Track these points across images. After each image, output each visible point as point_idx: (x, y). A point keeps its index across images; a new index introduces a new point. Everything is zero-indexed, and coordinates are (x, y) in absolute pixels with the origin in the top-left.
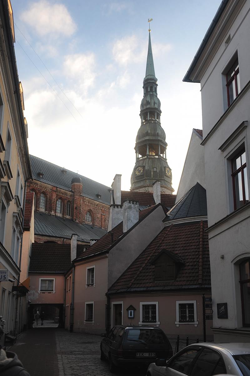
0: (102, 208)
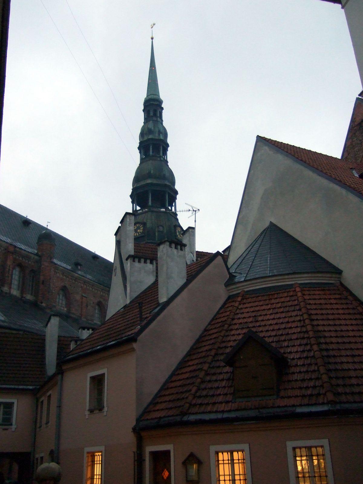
0: (82, 285)
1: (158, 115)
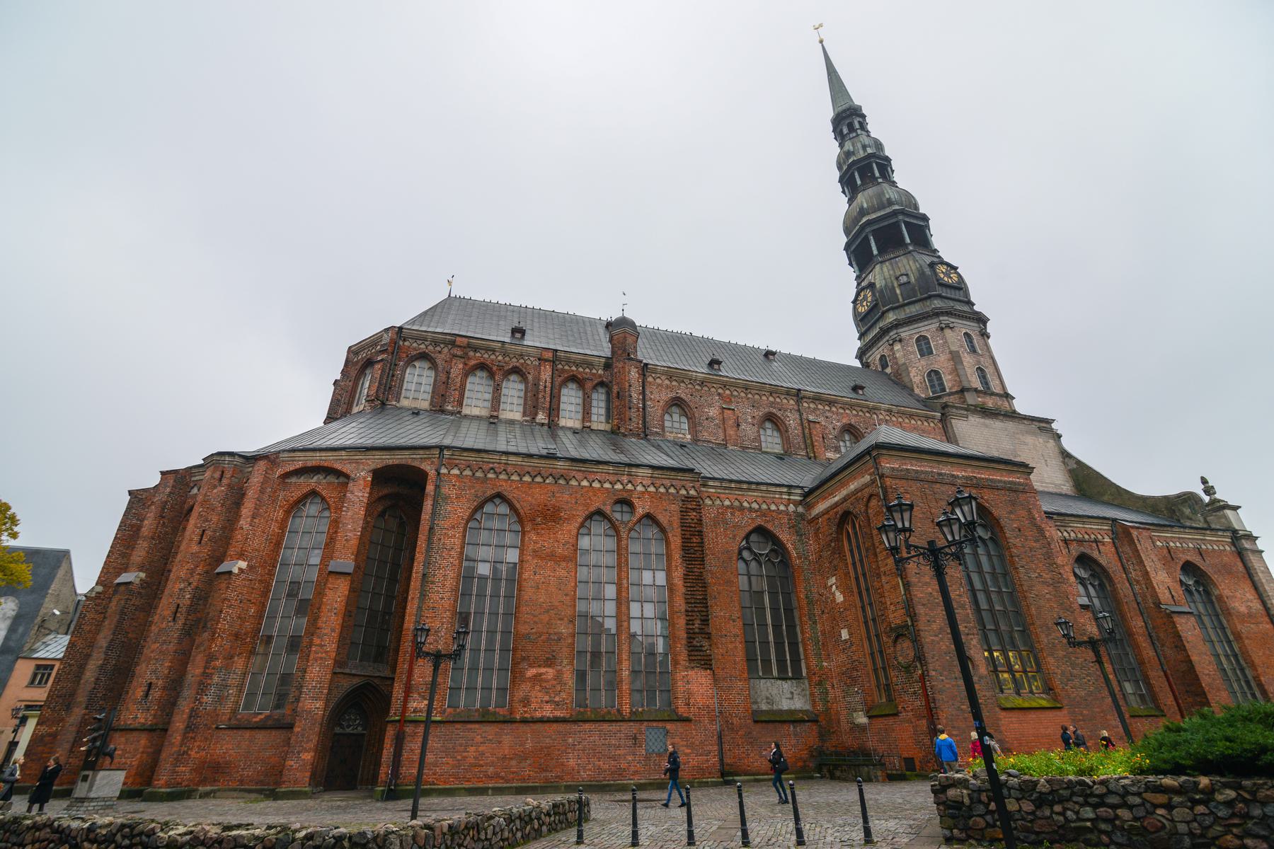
0: (720, 391)
1: (857, 126)
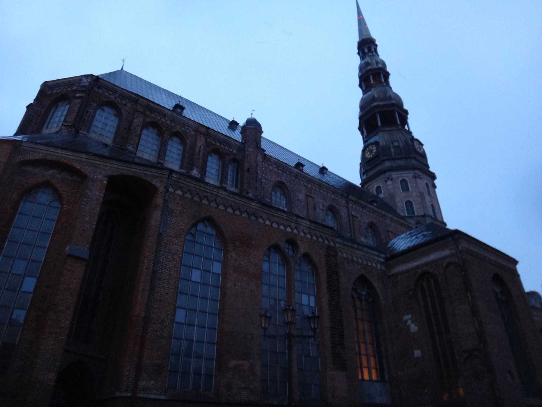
0: (306, 184)
1: (373, 50)
